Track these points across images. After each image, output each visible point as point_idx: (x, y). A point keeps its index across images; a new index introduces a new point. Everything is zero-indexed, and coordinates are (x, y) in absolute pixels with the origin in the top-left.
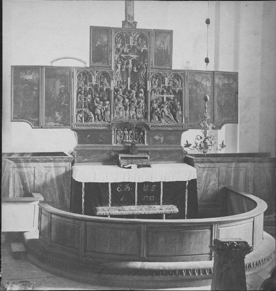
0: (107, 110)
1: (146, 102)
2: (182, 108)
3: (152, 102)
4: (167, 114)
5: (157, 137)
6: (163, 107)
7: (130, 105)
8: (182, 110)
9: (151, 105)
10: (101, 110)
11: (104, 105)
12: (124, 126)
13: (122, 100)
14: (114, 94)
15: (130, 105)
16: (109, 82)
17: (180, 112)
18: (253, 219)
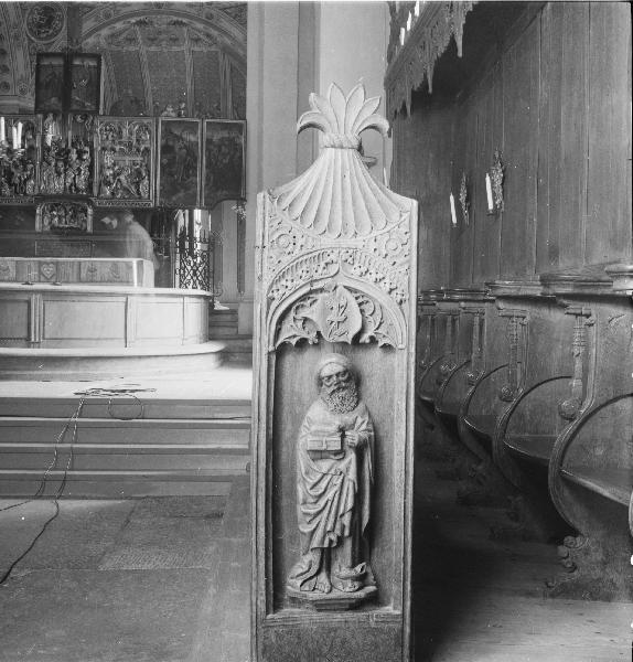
0: (29, 178)
1: (91, 168)
2: (149, 176)
3: (102, 167)
4: (125, 184)
5: (106, 220)
6: (119, 174)
7: (65, 170)
8: (149, 180)
9: (101, 172)
10: (20, 178)
11: (25, 170)
12: (54, 201)
13: (53, 163)
14: (43, 156)
15: (65, 170)
16: (34, 137)
17: (146, 182)
18: (124, 299)
